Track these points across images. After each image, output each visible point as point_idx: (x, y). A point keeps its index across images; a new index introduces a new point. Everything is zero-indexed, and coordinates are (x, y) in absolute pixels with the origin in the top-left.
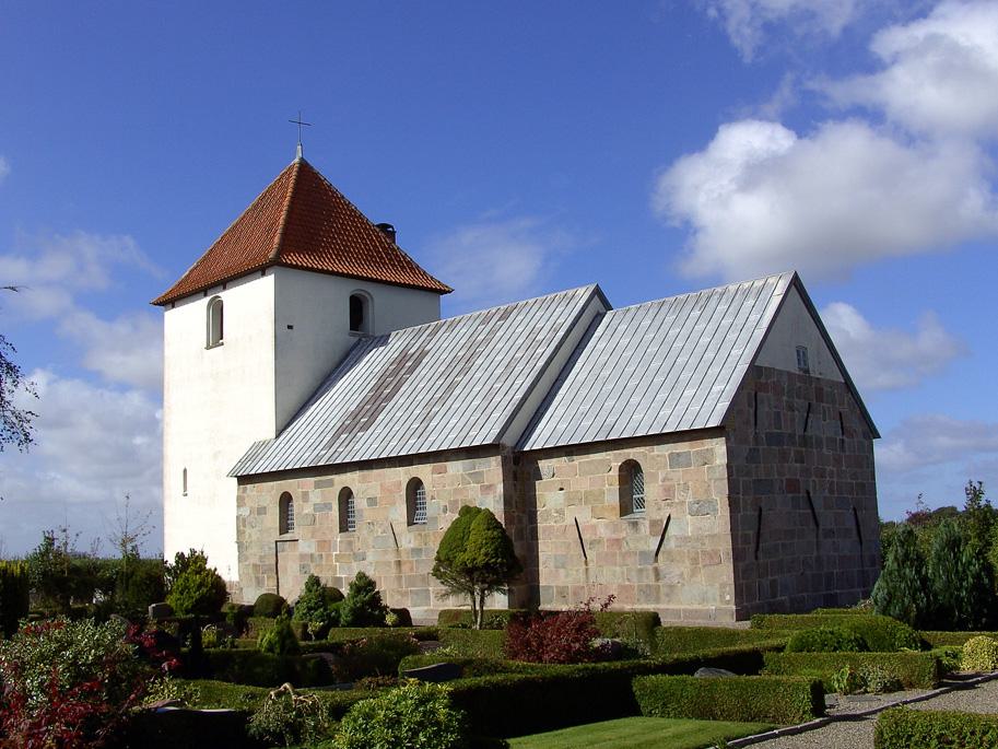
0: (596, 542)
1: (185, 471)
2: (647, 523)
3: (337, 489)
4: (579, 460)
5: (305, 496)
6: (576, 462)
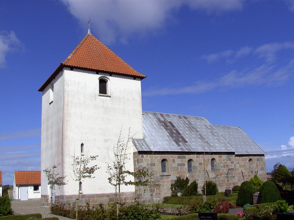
0: (246, 176)
1: (82, 145)
2: (254, 172)
3: (187, 160)
4: (241, 158)
5: (174, 161)
6: (241, 158)
